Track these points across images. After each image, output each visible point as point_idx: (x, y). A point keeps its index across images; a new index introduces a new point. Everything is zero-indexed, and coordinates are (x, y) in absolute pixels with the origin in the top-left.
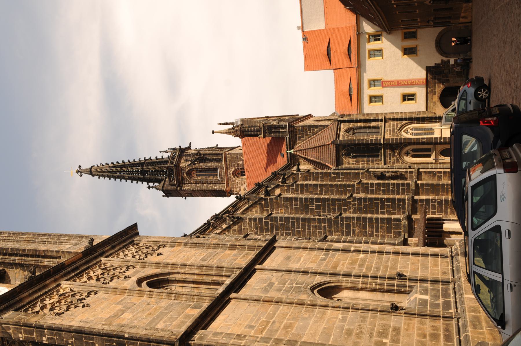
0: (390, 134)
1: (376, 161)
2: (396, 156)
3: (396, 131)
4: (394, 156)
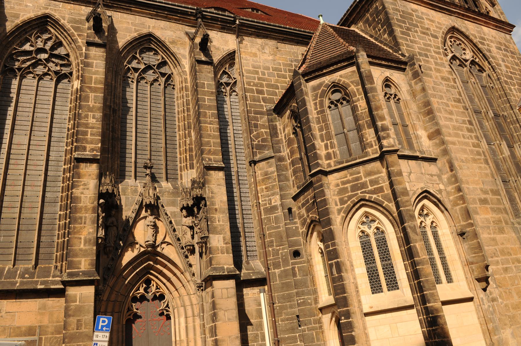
0: (344, 183)
1: (296, 178)
2: (308, 216)
3: (358, 194)
4: (308, 211)
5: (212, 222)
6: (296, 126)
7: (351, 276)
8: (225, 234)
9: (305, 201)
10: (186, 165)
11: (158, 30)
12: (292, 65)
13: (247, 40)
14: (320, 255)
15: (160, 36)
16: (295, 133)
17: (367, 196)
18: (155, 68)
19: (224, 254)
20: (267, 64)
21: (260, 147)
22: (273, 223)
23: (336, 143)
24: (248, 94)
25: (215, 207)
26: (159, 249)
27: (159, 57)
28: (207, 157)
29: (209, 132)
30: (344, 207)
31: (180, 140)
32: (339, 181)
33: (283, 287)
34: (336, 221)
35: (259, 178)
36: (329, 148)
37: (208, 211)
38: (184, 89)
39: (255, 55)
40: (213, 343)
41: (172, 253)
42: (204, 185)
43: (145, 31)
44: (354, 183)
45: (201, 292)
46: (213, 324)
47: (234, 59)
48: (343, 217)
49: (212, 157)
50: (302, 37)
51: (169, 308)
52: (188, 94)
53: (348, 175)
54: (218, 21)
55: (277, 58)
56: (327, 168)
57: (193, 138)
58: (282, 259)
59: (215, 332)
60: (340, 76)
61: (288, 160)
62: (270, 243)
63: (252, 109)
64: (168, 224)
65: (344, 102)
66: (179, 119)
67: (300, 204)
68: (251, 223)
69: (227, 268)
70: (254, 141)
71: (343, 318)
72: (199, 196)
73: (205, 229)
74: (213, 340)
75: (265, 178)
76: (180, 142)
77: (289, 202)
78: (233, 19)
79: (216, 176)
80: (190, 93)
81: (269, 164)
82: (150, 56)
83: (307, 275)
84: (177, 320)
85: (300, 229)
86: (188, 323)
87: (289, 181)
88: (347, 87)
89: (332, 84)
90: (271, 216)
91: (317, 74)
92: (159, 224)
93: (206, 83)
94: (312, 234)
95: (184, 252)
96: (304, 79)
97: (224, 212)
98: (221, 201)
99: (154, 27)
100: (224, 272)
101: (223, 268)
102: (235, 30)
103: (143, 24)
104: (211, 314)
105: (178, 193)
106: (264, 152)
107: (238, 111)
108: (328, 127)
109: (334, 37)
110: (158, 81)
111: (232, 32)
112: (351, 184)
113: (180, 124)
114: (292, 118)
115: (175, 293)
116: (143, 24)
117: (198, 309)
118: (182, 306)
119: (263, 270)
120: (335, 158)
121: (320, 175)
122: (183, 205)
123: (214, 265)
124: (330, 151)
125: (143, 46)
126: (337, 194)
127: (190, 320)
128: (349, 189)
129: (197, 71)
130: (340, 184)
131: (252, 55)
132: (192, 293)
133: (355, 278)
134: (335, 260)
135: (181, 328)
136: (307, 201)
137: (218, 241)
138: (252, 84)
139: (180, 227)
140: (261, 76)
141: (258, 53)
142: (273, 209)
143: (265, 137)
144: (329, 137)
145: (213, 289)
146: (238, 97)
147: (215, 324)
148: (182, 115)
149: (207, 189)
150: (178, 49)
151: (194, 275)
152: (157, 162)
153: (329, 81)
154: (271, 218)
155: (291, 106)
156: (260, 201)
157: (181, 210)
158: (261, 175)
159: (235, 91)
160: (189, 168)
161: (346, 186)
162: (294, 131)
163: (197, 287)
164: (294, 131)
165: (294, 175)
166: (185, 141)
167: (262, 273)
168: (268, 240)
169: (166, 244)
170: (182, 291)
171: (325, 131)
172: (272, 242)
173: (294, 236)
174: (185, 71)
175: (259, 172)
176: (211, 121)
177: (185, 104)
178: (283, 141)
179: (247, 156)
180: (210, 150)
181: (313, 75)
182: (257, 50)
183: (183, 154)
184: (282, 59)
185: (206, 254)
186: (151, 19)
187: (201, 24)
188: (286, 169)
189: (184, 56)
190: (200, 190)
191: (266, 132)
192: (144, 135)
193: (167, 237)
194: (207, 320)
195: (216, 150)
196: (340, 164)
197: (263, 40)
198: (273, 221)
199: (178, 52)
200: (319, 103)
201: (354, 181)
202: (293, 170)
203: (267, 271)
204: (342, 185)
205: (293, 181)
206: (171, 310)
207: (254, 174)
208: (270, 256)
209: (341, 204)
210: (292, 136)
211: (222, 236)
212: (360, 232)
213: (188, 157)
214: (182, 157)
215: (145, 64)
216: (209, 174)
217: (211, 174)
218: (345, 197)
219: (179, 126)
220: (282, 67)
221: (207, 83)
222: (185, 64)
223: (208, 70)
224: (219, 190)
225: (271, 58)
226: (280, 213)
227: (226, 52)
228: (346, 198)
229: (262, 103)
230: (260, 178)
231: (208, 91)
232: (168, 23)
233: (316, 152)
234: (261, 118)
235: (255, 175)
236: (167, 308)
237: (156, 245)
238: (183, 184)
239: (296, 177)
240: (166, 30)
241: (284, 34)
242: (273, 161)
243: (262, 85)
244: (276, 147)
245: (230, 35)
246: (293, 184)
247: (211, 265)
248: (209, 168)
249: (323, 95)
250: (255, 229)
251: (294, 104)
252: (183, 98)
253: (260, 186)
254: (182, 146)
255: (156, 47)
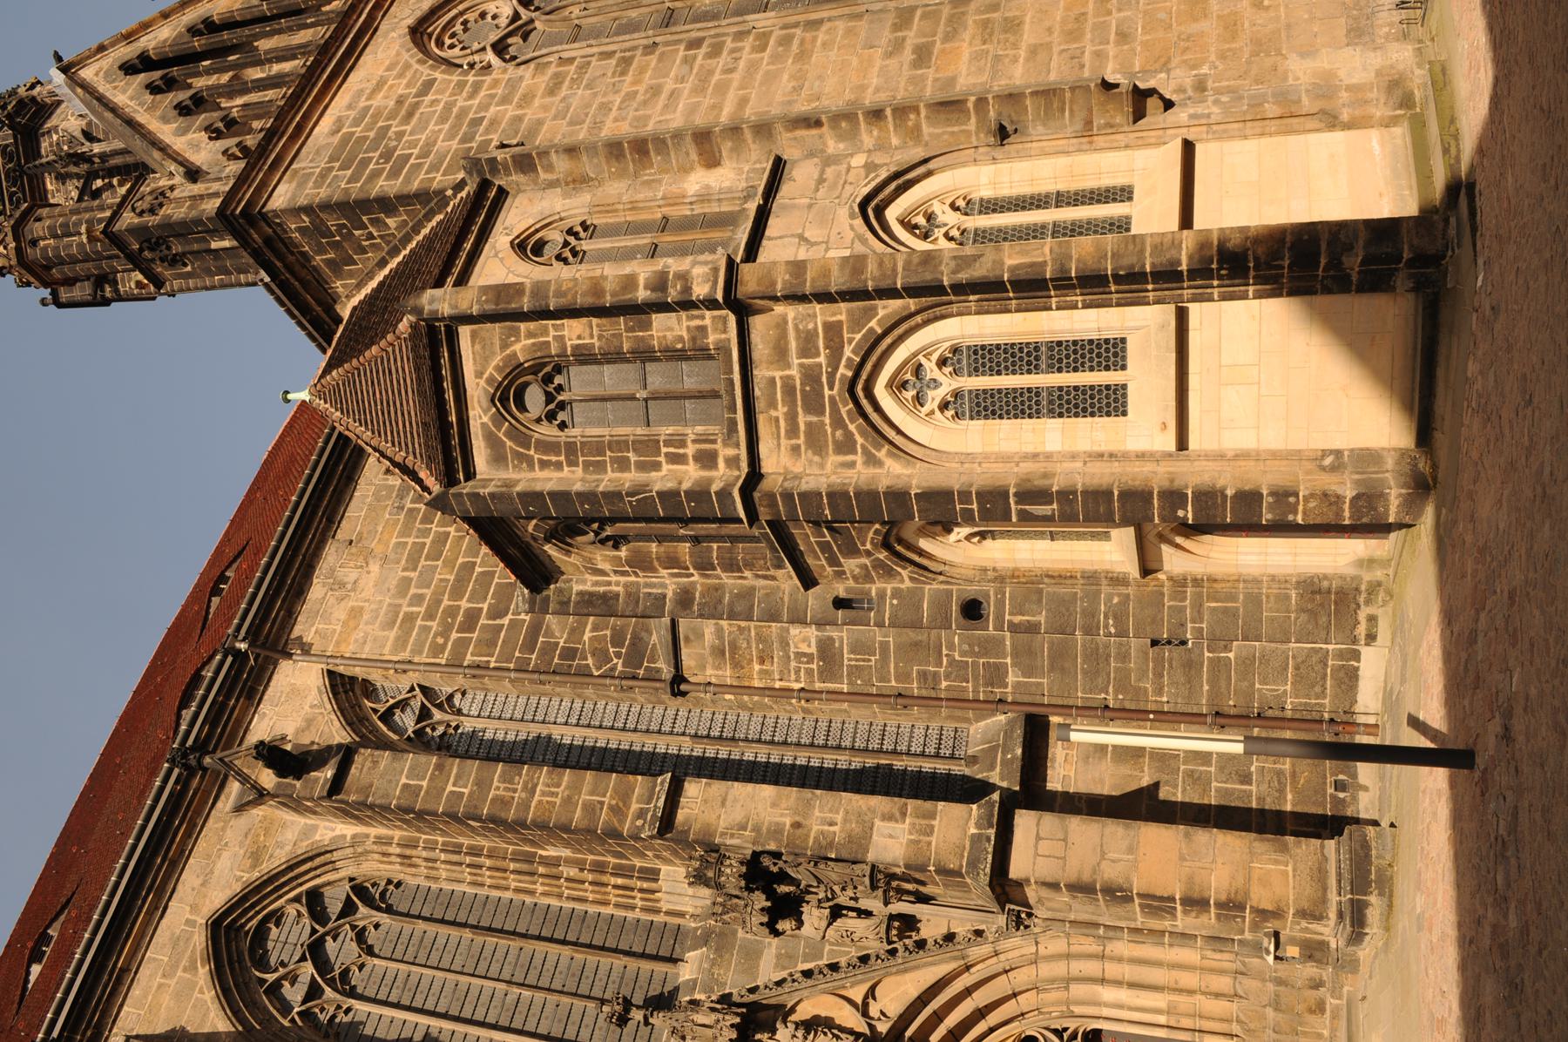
0: (793, 431)
1: (749, 565)
2: (868, 553)
3: (832, 398)
4: (852, 551)
5: (831, 845)
6: (597, 534)
7: (1065, 465)
8: (874, 812)
9: (823, 553)
10: (641, 890)
11: (205, 896)
12: (411, 510)
13: (306, 627)
14: (988, 543)
15: (228, 893)
16: (617, 541)
17: (844, 372)
18: (321, 930)
19: (932, 827)
20: (393, 583)
21: (637, 653)
22: (870, 660)
23: (670, 430)
24: (469, 657)
25: (788, 827)
26: (883, 1028)
27: (291, 910)
28: (633, 822)
29: (558, 801)
30: (862, 445)
31: (560, 896)
32: (784, 441)
33: (1063, 669)
34: (898, 476)
35: (727, 675)
36: (681, 451)
37: (797, 851)
38: (408, 852)
39: (356, 613)
40: (1194, 914)
41: (902, 989)
42: (713, 849)
43: (199, 939)
44: (799, 403)
45: (1036, 920)
46: (1137, 901)
47: (353, 679)
48: (890, 454)
49: (635, 806)
50: (336, 464)
51: (1065, 1029)
52: (426, 841)
53: (774, 413)
54: (224, 705)
55: (379, 550)
56: (739, 468)
57: (566, 853)
58: (978, 655)
59: (1161, 899)
60: (476, 377)
61: (692, 579)
62: (926, 680)
63: (517, 654)
64: (810, 982)
65: (558, 380)
66: (497, 887)
67: (829, 569)
68: (856, 728)
69: (978, 826)
70: (613, 669)
71: (1181, 513)
72: (744, 869)
73: (848, 871)
74: (1185, 912)
75: (732, 658)
76: (568, 898)
77: (815, 600)
78: (230, 659)
79: (693, 806)
80: (424, 837)
81: (692, 637)
82: (282, 938)
83: (1040, 592)
84: (1106, 1012)
85: (902, 586)
86: (1120, 978)
87: (753, 589)
88: (514, 363)
89: (495, 406)
90: (846, 662)
91: (455, 441)
92: (805, 1011)
93: (404, 780)
94: (921, 553)
95: (906, 949)
96: (463, 484)
97: (808, 804)
98: (774, 805)
99: (194, 908)
100: (988, 839)
101: (976, 839)
102: (267, 657)
103: (175, 942)
104: (1105, 900)
105: (721, 935)
106: (654, 645)
107: (512, 699)
108: (618, 442)
109: (358, 369)
110: (364, 928)
111: (267, 668)
112: (800, 410)
113: (513, 885)
114: (569, 540)
115: (1026, 1002)
116: (175, 942)
117: (1083, 940)
118: (1067, 988)
119: (1002, 718)
120: (714, 442)
121: (756, 495)
122: (762, 924)
123: (961, 866)
124: (690, 450)
125: (246, 953)
126: (820, 455)
127: (1112, 970)
128: (814, 419)
129: (362, 799)
130: (794, 442)
131: (352, 624)
132: (1033, 949)
133: (1073, 456)
134: (1012, 501)
135: (1132, 1005)
136: (825, 547)
137: (891, 836)
138: (440, 640)
139: (827, 948)
140: (423, 610)
141: (351, 604)
142: (827, 652)
143: (608, 633)
144: (649, 446)
145: (1032, 881)
146: (469, 691)
147: (1138, 894)
148: (488, 873)
149: (729, 842)
150: (280, 845)
151: (979, 933)
152: (614, 982)
153: (485, 412)
154: (853, 663)
155: (535, 539)
156: (797, 686)
157: (776, 933)
158: (718, 668)
159: (450, 697)
160: (653, 886)
161: (802, 427)
162: (611, 543)
163: (1018, 929)
164: (611, 543)
165: (740, 570)
166: (568, 880)
167: (1010, 722)
168: (915, 685)
169: (871, 1001)
170: (1020, 978)
171: (630, 455)
172: (923, 675)
173: (919, 607)
174: (354, 836)
175: (709, 671)
176: (525, 788)
177: (455, 858)
178: (632, 583)
179: (653, 699)
180: (611, 808)
181: (457, 454)
182: (343, 603)
183: (605, 893)
184: (386, 536)
185: (923, 883)
186: (168, 911)
187: (221, 759)
188: (717, 590)
189: (308, 832)
190: (728, 862)
191: (594, 629)
192: (522, 1008)
193: (851, 993)
194: (1120, 919)
195: (615, 790)
196: (736, 431)
197: (315, 581)
198: (864, 660)
199: (288, 848)
200: (544, 453)
201: (794, 402)
202: (724, 571)
203: (1007, 707)
204: (799, 438)
205: (758, 576)
206: (1072, 1025)
207: (712, 688)
208: (965, 690)
209: (854, 452)
210: (623, 552)
211: (878, 823)
212: (942, 412)
213: (620, 881)
214: (614, 900)
215: (303, 959)
216: (683, 824)
217: (687, 821)
218: (833, 435)
219: (517, 890)
220: (411, 540)
221: (407, 778)
222: (330, 834)
223: (368, 764)
224: (739, 805)
225: (375, 568)
226: (842, 635)
227: (326, 699)
228: (839, 433)
229: (506, 621)
230: (728, 673)
231: (431, 779)
232: (191, 860)
233: (685, 492)
234: (549, 633)
235: (715, 685)
236: (1066, 1036)
237: (868, 1032)
238: (699, 911)
239: (746, 565)
240: (212, 872)
241: (314, 513)
242: (684, 625)
243: (452, 612)
244: (646, 607)
245: (275, 677)
246: (765, 577)
247: (958, 874)
248: (667, 822)
249: (524, 440)
250: (875, 717)
251: (530, 529)
252: (435, 861)
253: (751, 678)
254: (581, 893)
255: (258, 913)
